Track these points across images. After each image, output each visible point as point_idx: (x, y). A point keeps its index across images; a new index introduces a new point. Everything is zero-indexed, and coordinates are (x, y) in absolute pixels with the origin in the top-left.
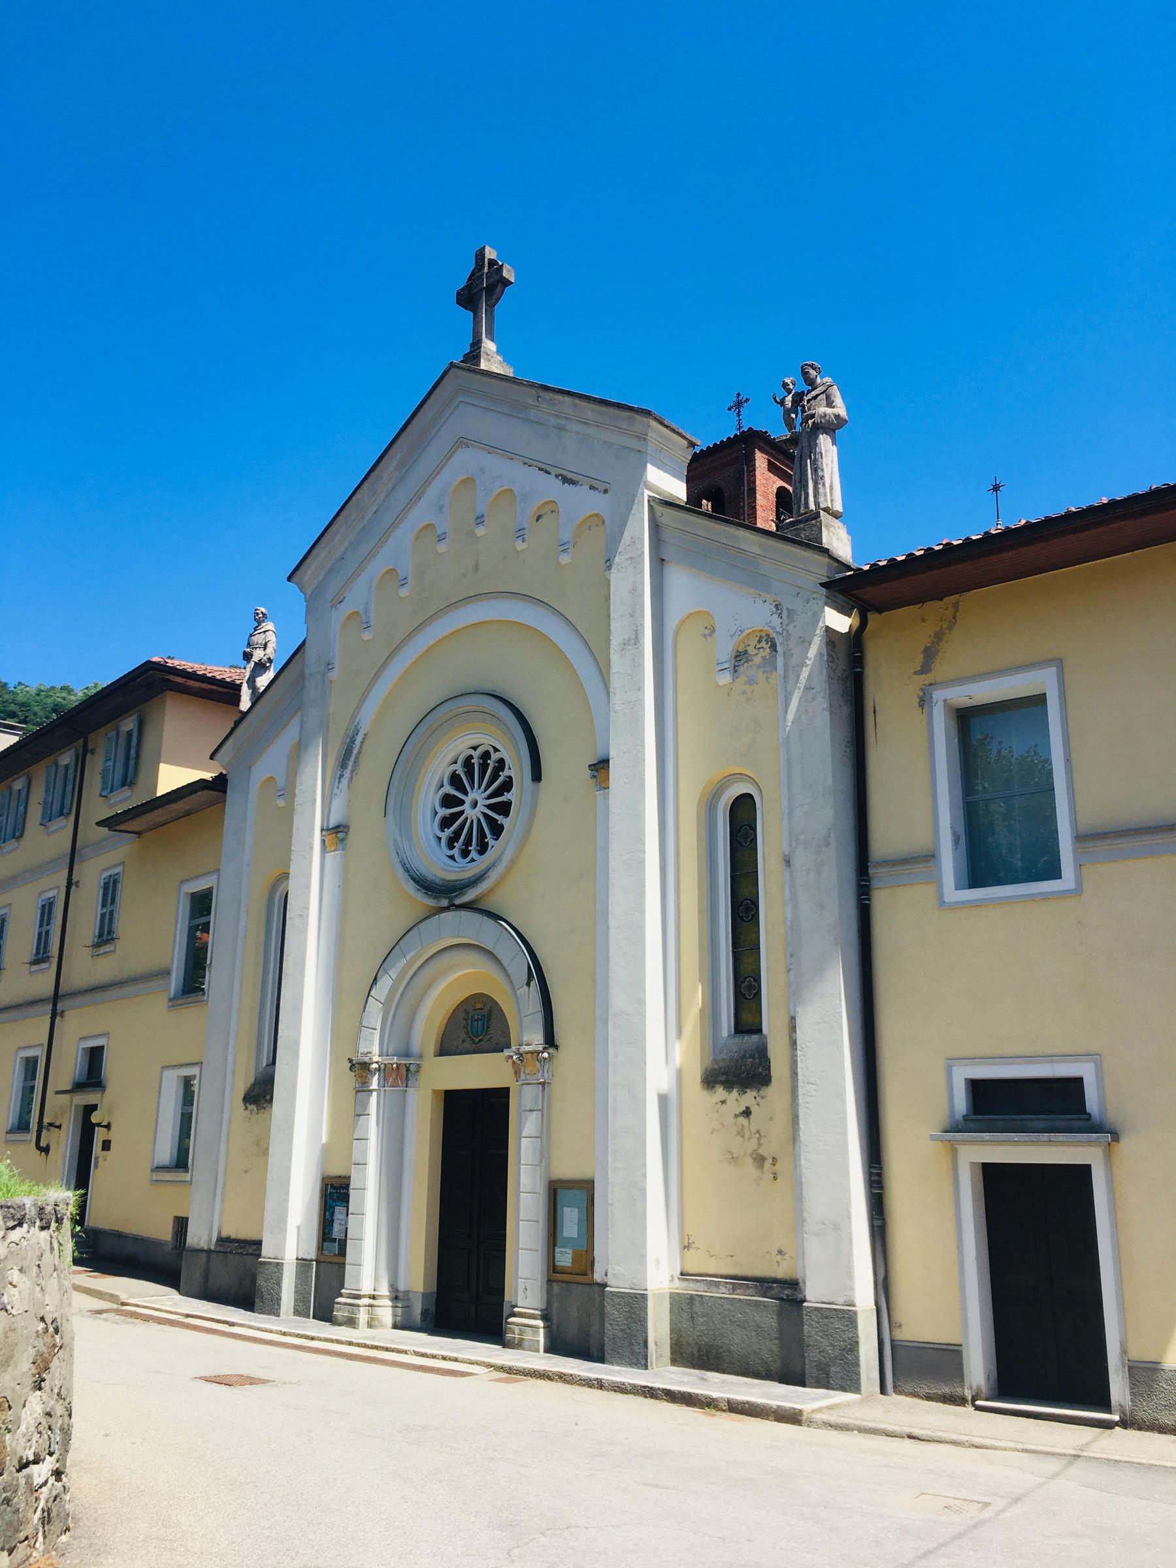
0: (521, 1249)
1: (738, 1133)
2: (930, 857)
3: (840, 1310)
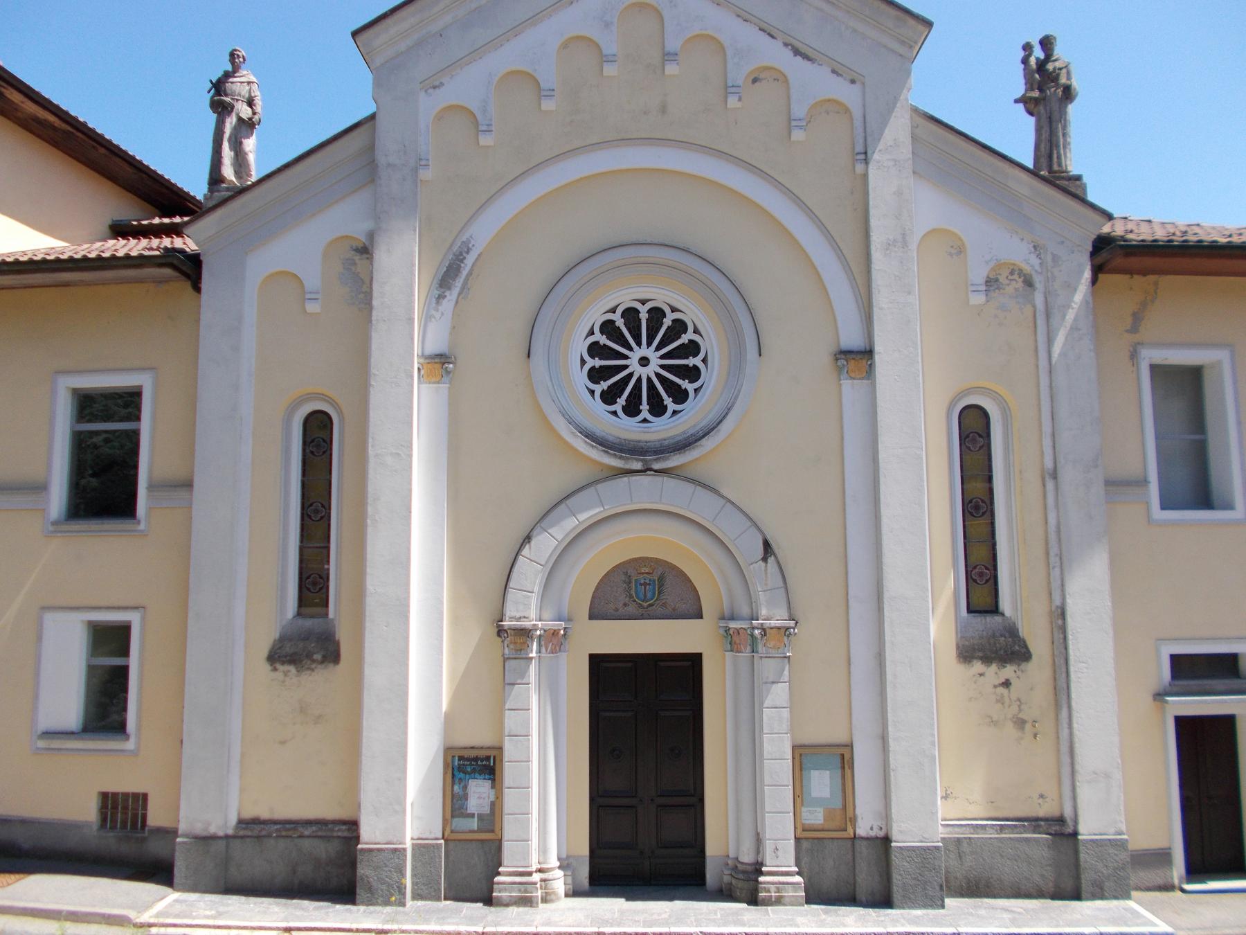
0: (768, 813)
1: (998, 701)
2: (1143, 482)
3: (1113, 840)
